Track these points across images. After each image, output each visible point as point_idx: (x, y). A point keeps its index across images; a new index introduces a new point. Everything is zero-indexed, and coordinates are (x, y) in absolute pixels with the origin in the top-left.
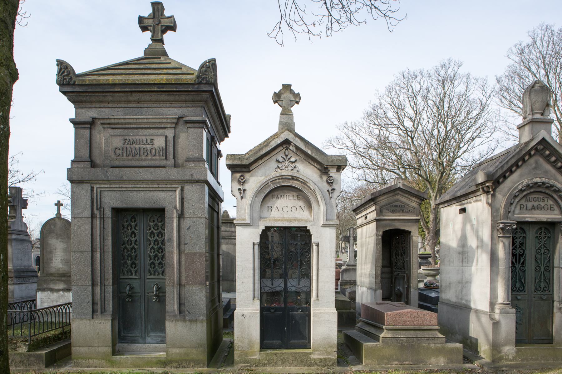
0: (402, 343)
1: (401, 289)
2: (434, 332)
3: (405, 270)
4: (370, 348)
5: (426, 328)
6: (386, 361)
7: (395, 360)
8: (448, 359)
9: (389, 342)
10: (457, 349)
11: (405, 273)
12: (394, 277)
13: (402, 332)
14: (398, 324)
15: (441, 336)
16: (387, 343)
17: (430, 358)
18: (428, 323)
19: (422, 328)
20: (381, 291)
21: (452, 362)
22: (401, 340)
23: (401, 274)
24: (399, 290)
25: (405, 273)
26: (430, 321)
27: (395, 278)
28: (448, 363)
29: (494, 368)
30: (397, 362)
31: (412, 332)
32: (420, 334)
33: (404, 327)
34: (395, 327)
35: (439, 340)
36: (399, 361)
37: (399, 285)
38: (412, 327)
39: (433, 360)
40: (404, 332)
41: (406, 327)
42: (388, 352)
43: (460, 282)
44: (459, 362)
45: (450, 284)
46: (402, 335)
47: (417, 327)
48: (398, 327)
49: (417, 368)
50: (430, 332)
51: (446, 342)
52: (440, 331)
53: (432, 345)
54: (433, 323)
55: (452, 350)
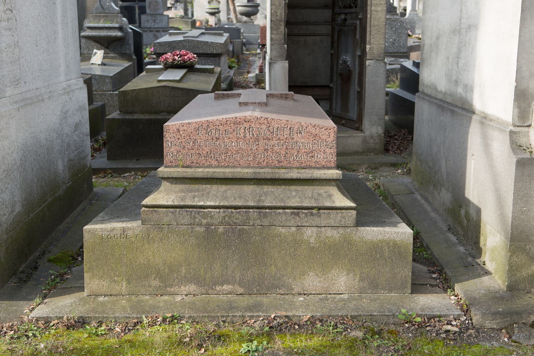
0: (208, 226)
1: (348, 58)
2: (322, 190)
3: (358, 10)
4: (103, 240)
5: (294, 174)
6: (155, 283)
7: (188, 280)
8: (362, 280)
9: (166, 220)
10: (395, 247)
11: (357, 18)
12: (337, 28)
13: (215, 188)
14: (202, 160)
15: (341, 200)
16: (159, 226)
17: (304, 273)
18: (304, 158)
19: (283, 174)
20: (286, 64)
21: (374, 285)
22: (205, 216)
23: (349, 22)
24: (345, 62)
25: (357, 18)
26: (311, 153)
27: (340, 31)
28: (362, 291)
29: (503, 315)
30: (192, 288)
31: (248, 189)
32: (272, 196)
33: (220, 172)
34: (190, 172)
35: (335, 218)
36: (197, 280)
37: (347, 51)
38: (247, 172)
39: (312, 281)
40: (223, 188)
41: (228, 172)
42: (164, 252)
43: (456, 31)
44: (400, 288)
45: (438, 38)
46: (212, 197)
47: (266, 173)
48: (200, 172)
49: (250, 308)
50: (309, 190)
51: (360, 223)
52: (345, 186)
53: (310, 233)
54: (320, 158)
55: (376, 250)
